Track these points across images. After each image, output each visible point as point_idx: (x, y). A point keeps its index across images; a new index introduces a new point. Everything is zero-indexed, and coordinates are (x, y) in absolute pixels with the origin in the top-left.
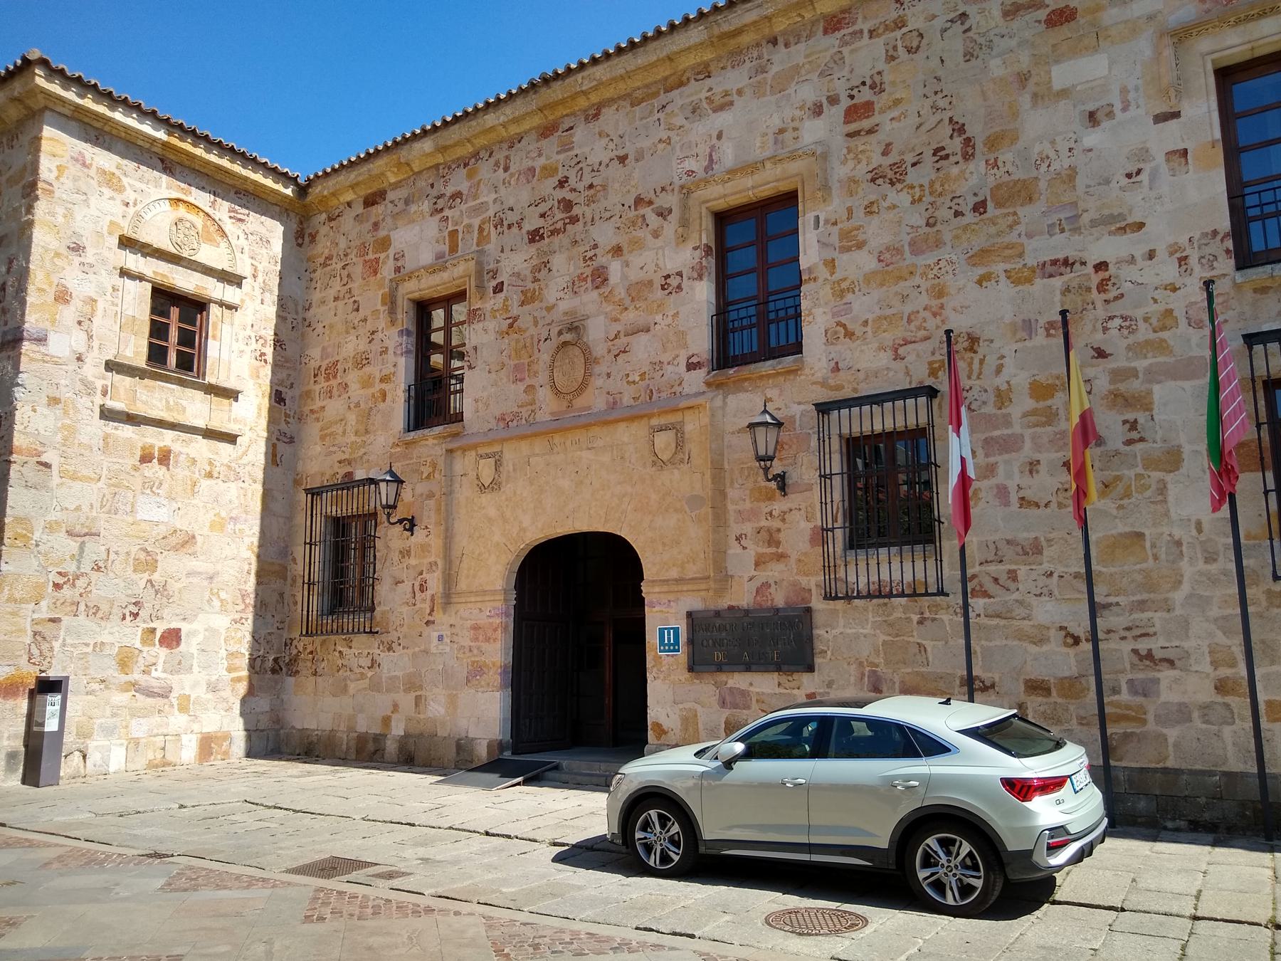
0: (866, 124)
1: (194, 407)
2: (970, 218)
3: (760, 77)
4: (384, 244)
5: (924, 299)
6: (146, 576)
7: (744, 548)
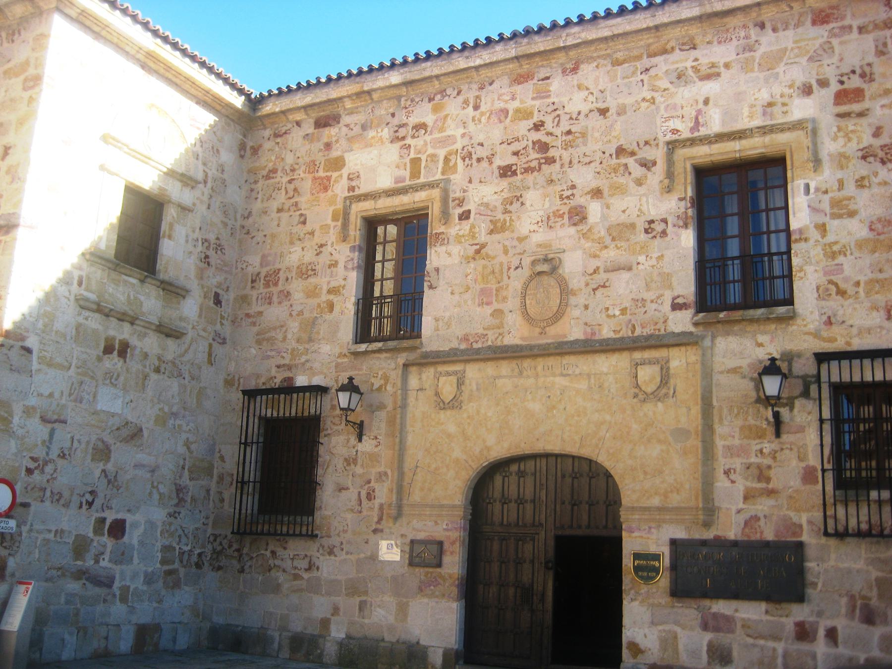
0: (856, 107)
3: (747, 55)
4: (338, 164)
6: (101, 466)
7: (733, 482)
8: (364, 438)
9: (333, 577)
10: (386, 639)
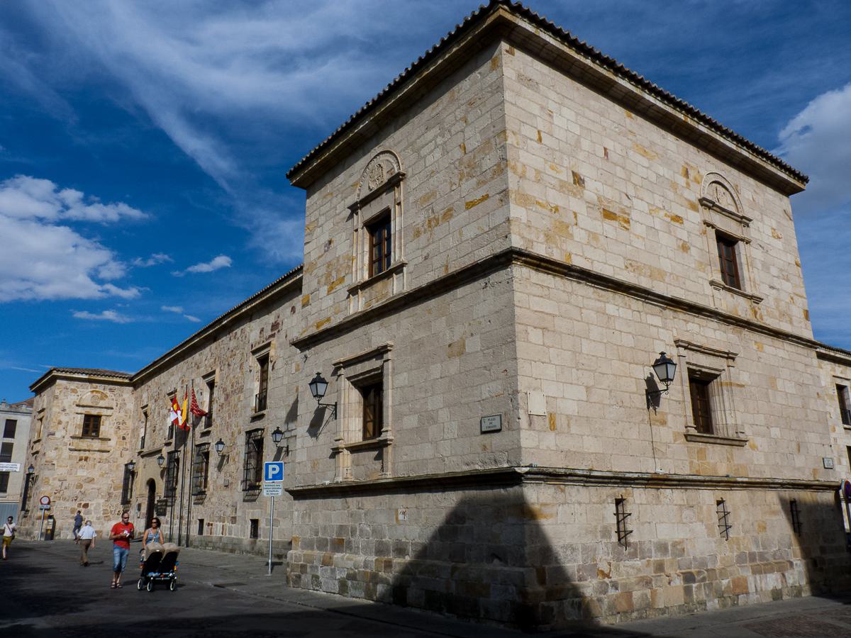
1: (96, 444)
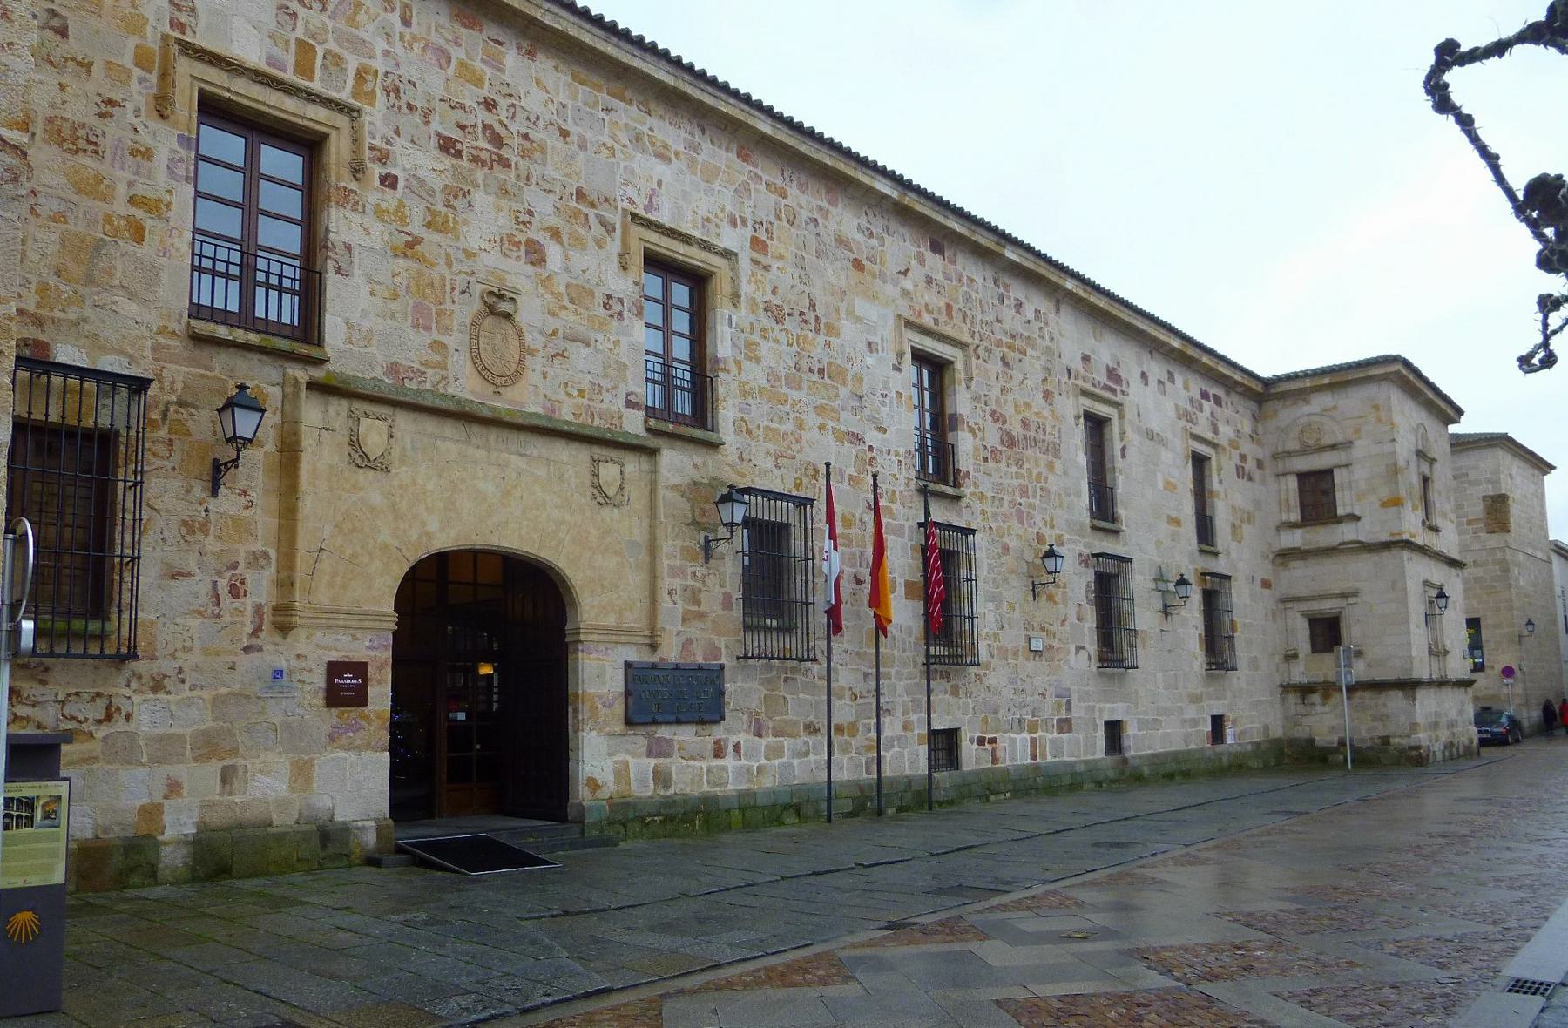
2: (815, 377)
5: (789, 427)
8: (222, 490)
9: (160, 730)
10: (276, 823)
